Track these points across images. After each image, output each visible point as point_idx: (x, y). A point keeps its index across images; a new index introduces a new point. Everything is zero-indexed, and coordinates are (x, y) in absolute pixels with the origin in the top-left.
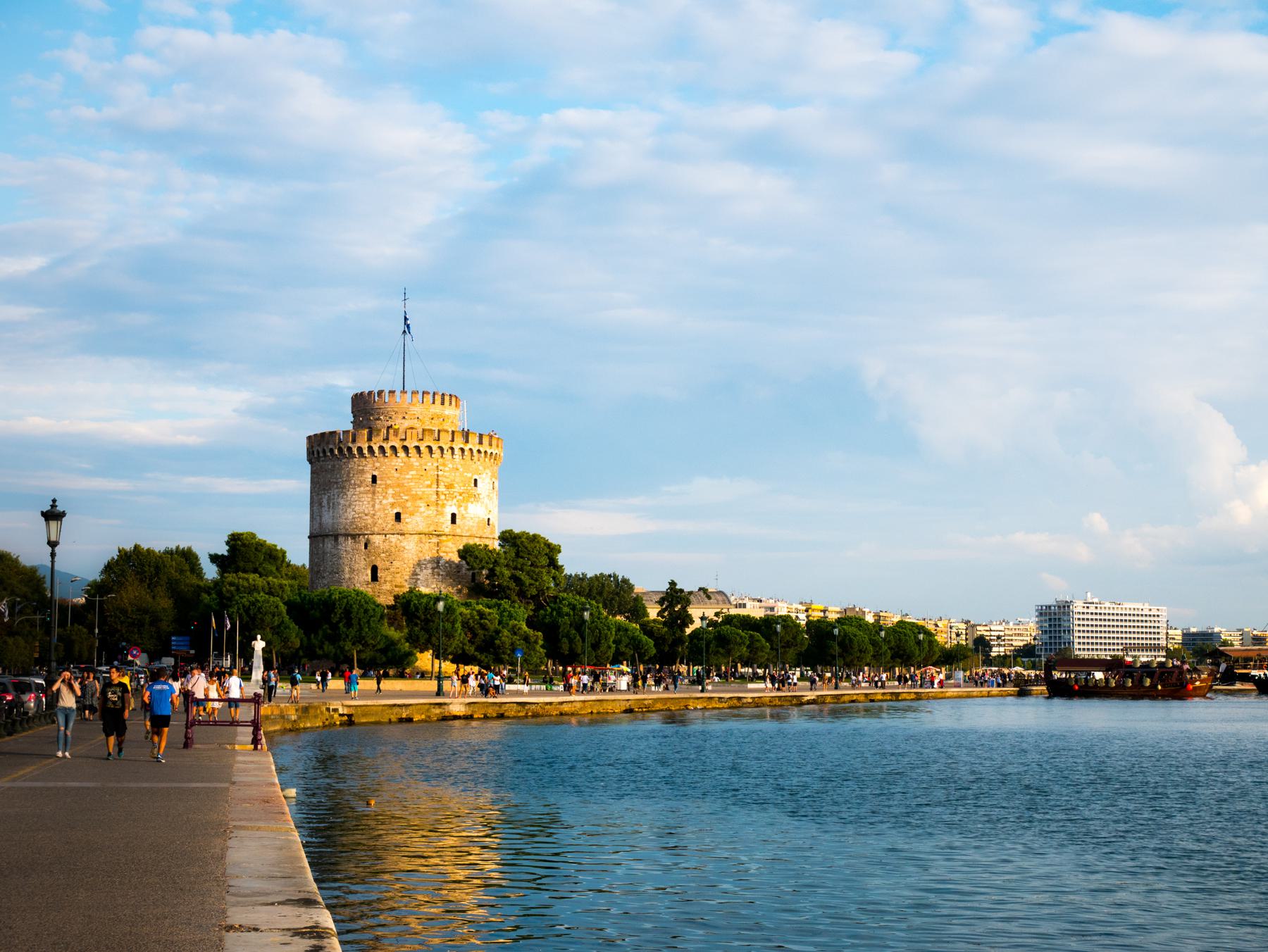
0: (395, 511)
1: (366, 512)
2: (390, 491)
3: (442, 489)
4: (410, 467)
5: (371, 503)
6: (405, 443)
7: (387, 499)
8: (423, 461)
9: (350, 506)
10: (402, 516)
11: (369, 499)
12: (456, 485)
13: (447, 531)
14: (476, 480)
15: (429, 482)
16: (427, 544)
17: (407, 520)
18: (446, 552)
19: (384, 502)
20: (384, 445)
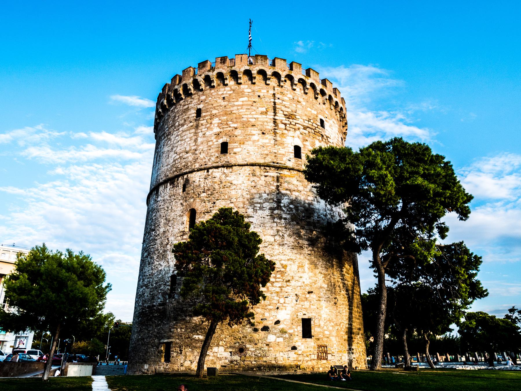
0: (221, 141)
1: (188, 149)
2: (216, 121)
3: (280, 117)
4: (241, 94)
5: (194, 138)
6: (233, 68)
7: (212, 129)
8: (255, 88)
9: (172, 149)
10: (230, 146)
11: (192, 135)
12: (297, 117)
13: (290, 164)
14: (322, 122)
15: (264, 109)
16: (263, 178)
17: (235, 150)
18: (290, 190)
19: (208, 133)
20: (210, 74)
